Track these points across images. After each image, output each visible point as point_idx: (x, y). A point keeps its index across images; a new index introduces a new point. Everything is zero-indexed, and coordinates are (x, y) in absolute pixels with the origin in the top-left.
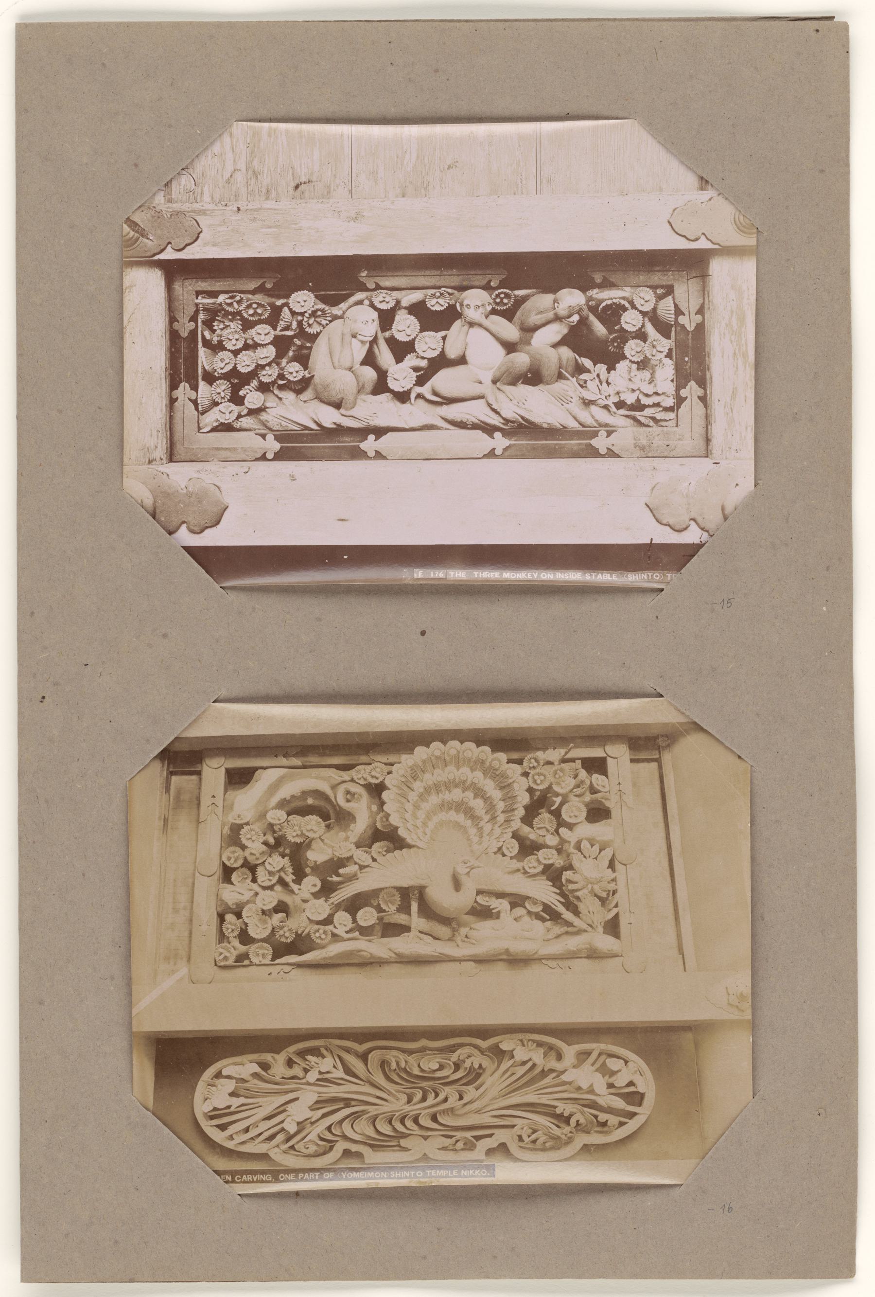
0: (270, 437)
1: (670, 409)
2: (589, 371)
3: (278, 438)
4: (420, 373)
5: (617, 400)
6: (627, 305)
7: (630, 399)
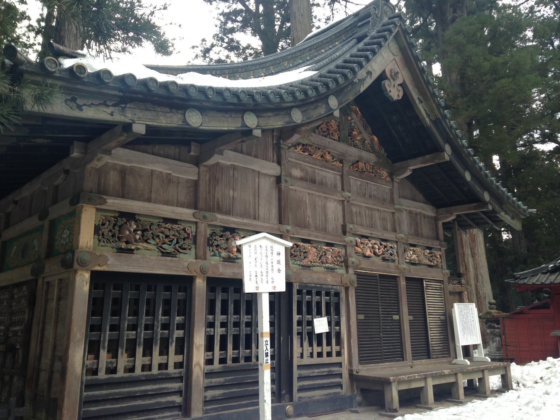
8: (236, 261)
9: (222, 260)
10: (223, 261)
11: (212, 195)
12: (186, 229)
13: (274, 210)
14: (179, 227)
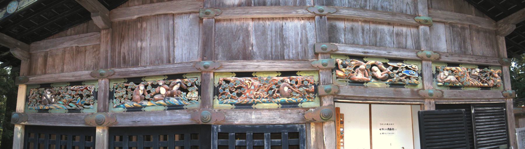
0: (125, 108)
1: (197, 100)
2: (182, 94)
5: (188, 99)
8: (143, 109)
9: (127, 110)
10: (127, 111)
11: (118, 52)
12: (88, 88)
13: (197, 48)
14: (82, 87)
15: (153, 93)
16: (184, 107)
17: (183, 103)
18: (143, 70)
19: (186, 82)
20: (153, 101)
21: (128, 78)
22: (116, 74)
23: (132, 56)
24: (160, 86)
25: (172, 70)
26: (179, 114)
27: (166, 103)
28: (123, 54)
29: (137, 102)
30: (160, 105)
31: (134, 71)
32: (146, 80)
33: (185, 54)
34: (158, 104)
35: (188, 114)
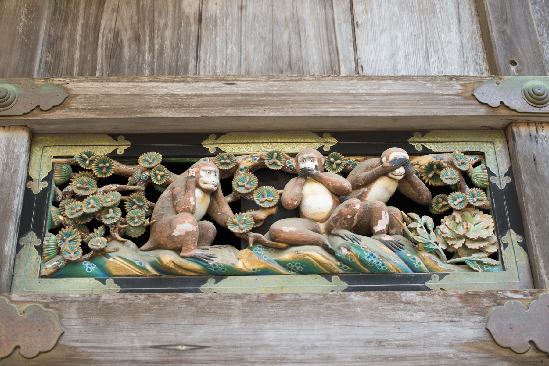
0: (110, 281)
1: (494, 256)
3: (117, 282)
4: (259, 225)
5: (444, 248)
6: (445, 165)
7: (458, 245)
8: (210, 286)
11: (86, 25)
13: (454, 35)
15: (264, 209)
16: (428, 284)
17: (422, 265)
18: (221, 95)
19: (430, 167)
20: (267, 247)
21: (128, 137)
22: (74, 104)
23: (156, 47)
24: (306, 175)
25: (365, 103)
26: (420, 316)
27: (338, 259)
28: (110, 36)
29: (178, 250)
30: (300, 273)
31: (174, 95)
32: (229, 149)
33: (406, 57)
34: (294, 260)
35: (472, 314)
